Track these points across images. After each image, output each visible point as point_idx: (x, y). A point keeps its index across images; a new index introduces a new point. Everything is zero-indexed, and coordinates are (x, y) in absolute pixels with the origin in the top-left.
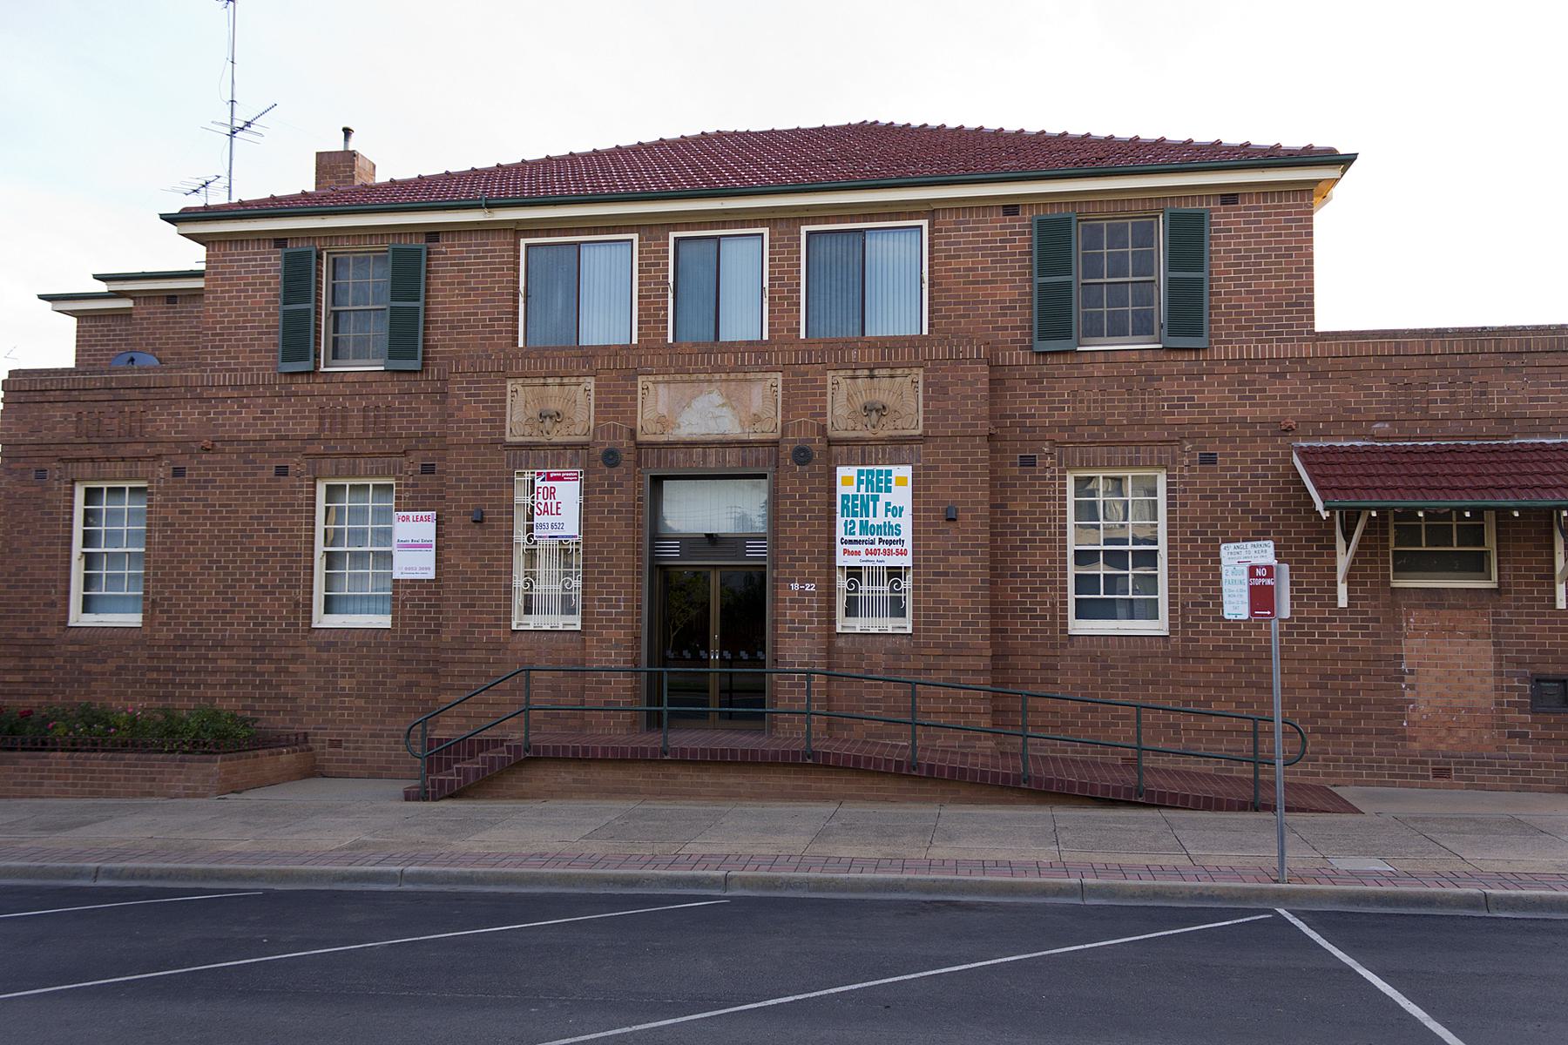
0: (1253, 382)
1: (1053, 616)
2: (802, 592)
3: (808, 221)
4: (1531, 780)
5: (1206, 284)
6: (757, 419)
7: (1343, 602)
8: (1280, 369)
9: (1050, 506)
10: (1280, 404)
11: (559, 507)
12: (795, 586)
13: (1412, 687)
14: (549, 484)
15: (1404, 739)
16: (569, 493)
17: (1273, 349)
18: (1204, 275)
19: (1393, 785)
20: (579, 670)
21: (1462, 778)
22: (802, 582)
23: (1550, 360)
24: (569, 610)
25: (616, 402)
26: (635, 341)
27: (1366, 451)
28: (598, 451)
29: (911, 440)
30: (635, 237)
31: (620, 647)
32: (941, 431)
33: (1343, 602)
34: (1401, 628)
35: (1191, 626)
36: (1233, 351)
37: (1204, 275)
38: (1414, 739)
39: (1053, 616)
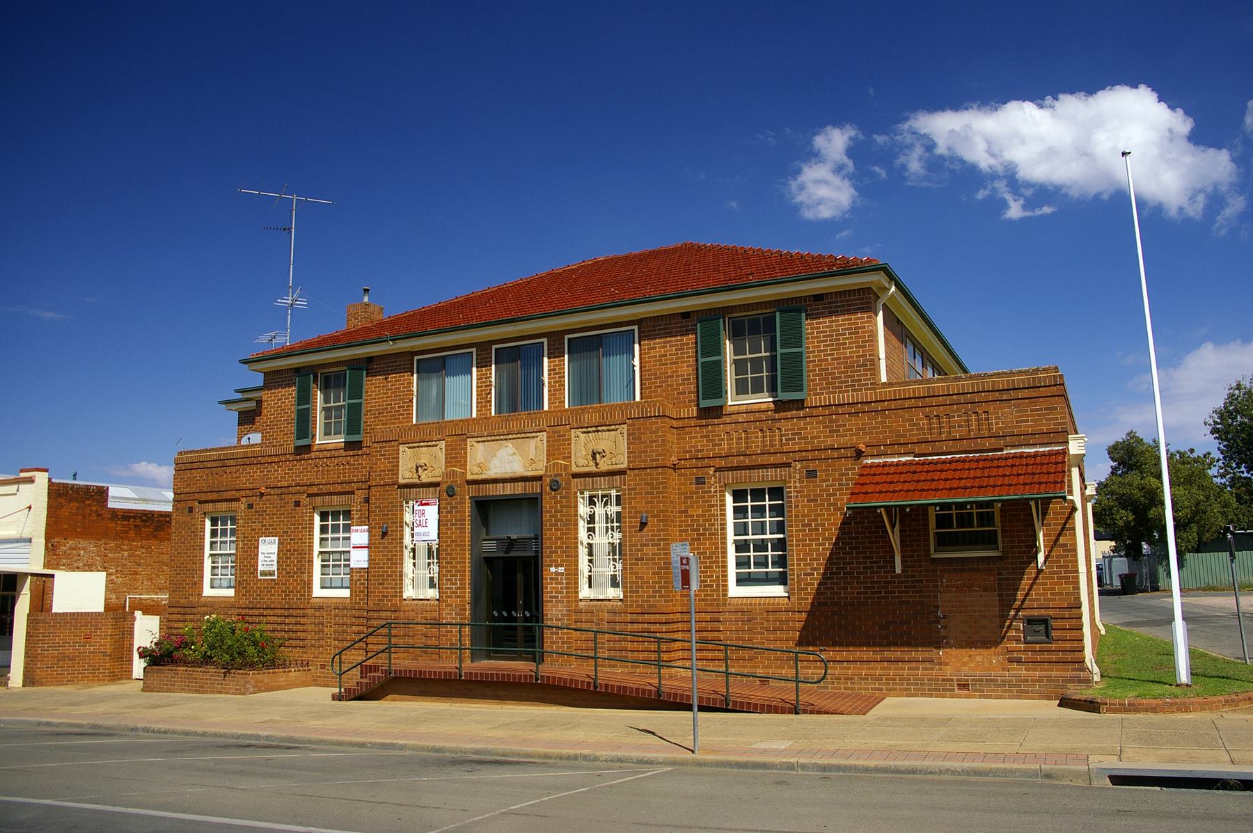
0: (838, 420)
1: (718, 586)
2: (556, 573)
3: (496, 342)
4: (1022, 691)
5: (805, 356)
6: (533, 461)
7: (898, 570)
8: (855, 408)
9: (714, 511)
10: (855, 435)
11: (424, 523)
12: (553, 569)
13: (945, 627)
14: (422, 508)
15: (940, 664)
16: (432, 512)
17: (850, 397)
18: (803, 350)
19: (931, 696)
20: (437, 624)
21: (976, 691)
22: (557, 567)
23: (1027, 393)
24: (432, 585)
25: (456, 456)
26: (474, 416)
27: (910, 463)
28: (444, 487)
29: (621, 472)
30: (474, 350)
31: (460, 609)
32: (637, 464)
33: (898, 570)
34: (937, 586)
35: (803, 589)
36: (825, 399)
37: (803, 350)
38: (947, 664)
39: (718, 586)
